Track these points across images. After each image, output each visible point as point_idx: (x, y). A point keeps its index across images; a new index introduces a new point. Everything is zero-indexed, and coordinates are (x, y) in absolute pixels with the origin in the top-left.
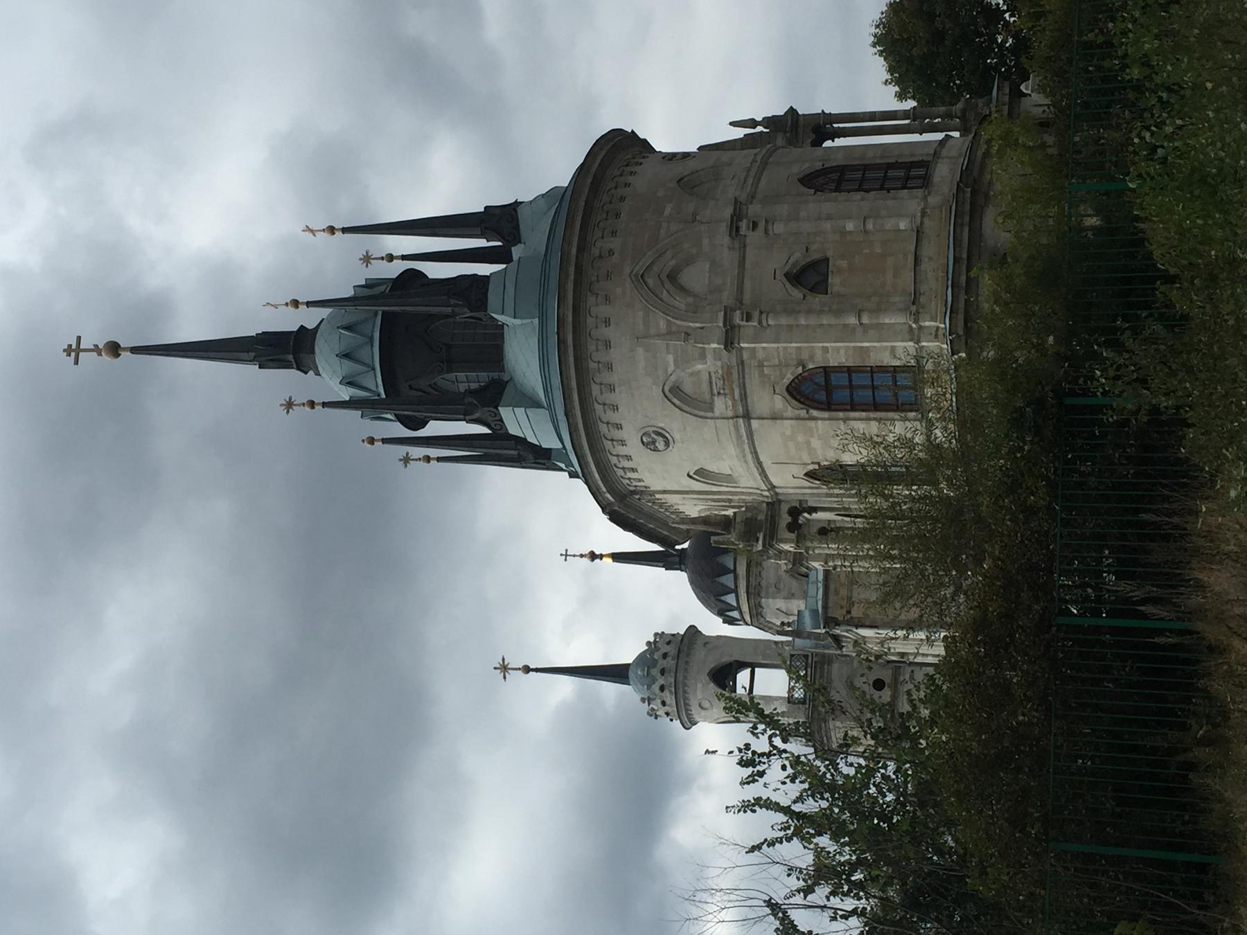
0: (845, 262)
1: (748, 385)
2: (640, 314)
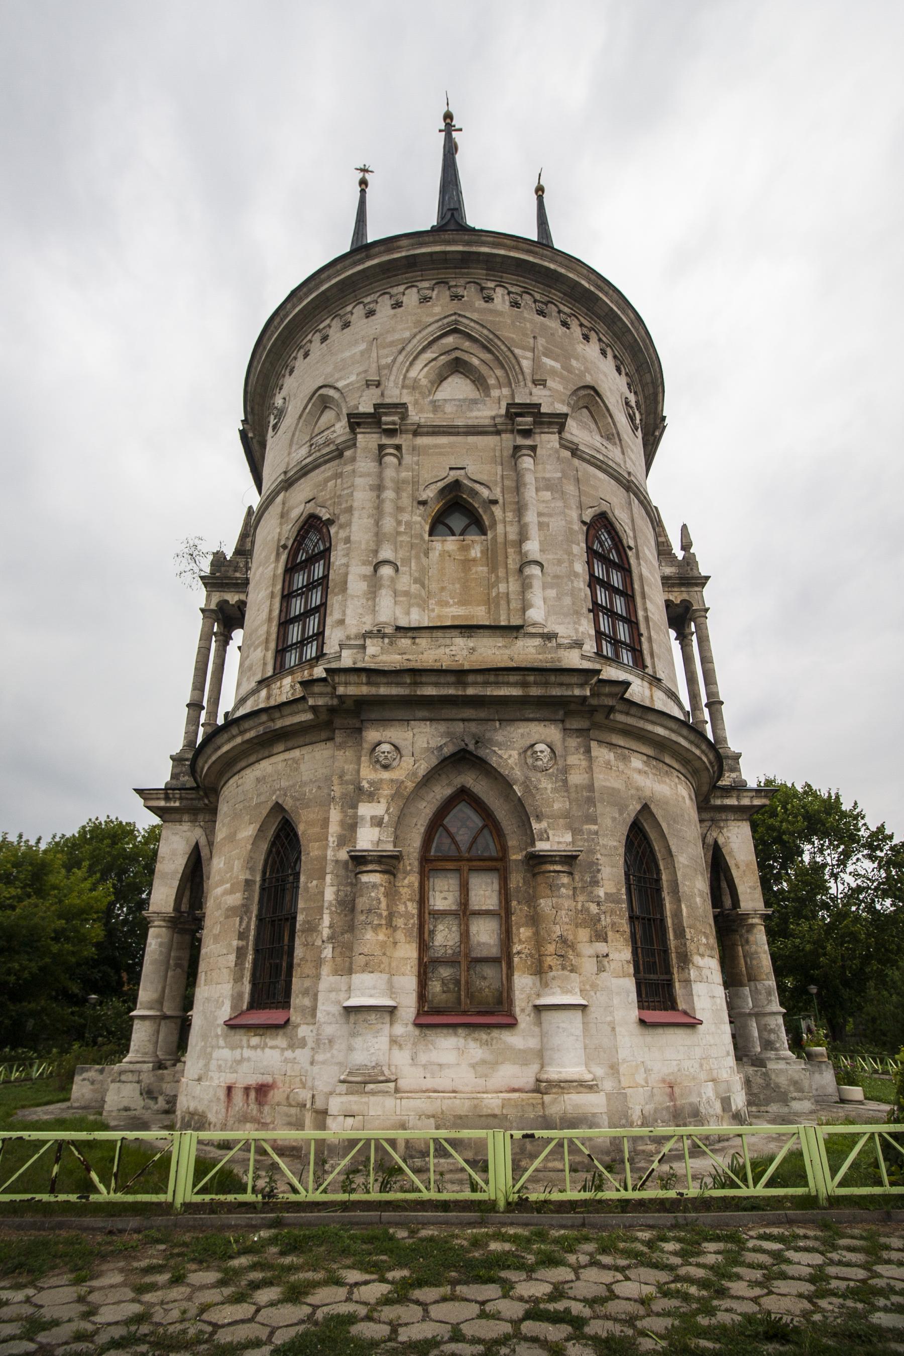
0: (479, 555)
1: (317, 471)
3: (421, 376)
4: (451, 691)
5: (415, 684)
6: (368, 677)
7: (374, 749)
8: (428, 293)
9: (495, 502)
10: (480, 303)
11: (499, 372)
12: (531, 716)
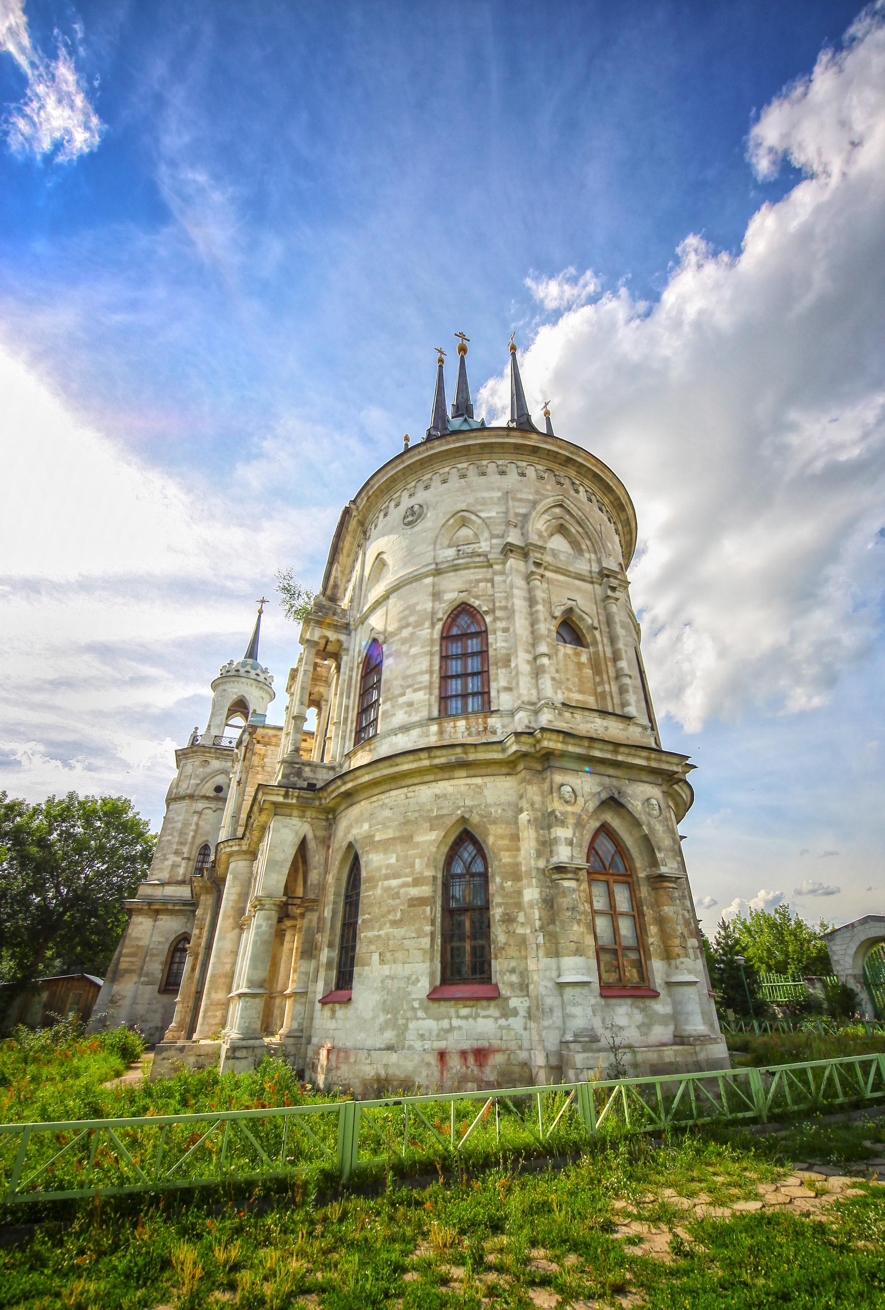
1: (467, 571)
2: (531, 497)
3: (543, 529)
4: (609, 756)
5: (590, 747)
6: (564, 738)
7: (560, 788)
8: (542, 474)
9: (596, 629)
10: (572, 492)
11: (588, 543)
12: (645, 779)
